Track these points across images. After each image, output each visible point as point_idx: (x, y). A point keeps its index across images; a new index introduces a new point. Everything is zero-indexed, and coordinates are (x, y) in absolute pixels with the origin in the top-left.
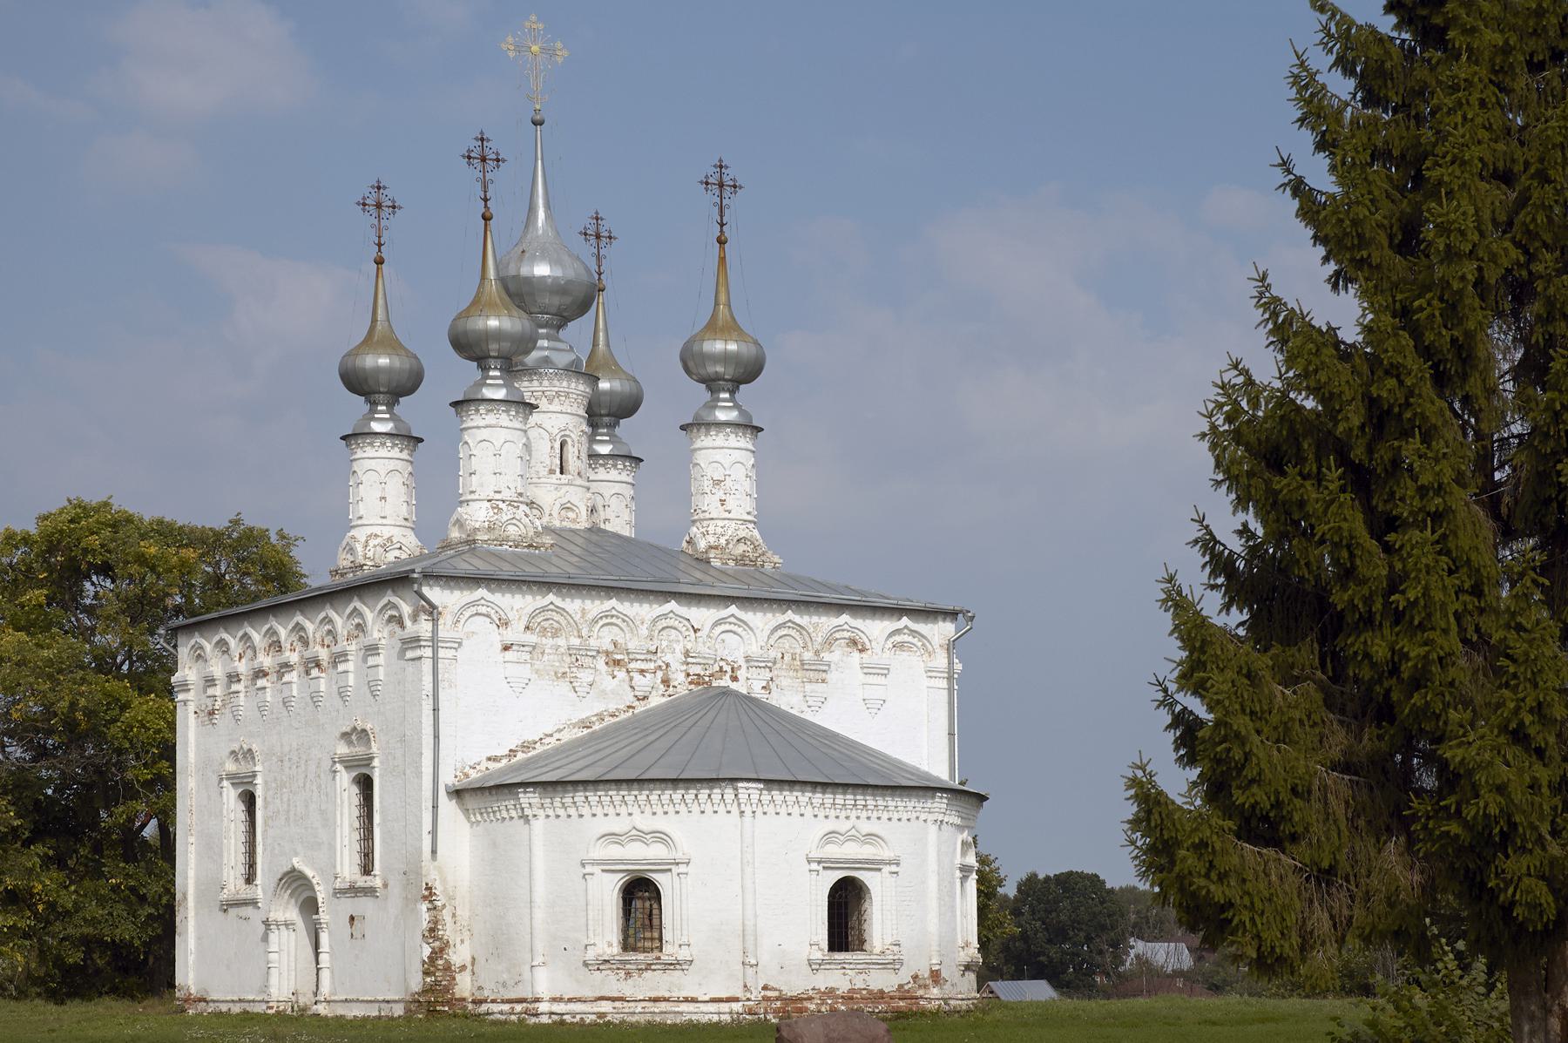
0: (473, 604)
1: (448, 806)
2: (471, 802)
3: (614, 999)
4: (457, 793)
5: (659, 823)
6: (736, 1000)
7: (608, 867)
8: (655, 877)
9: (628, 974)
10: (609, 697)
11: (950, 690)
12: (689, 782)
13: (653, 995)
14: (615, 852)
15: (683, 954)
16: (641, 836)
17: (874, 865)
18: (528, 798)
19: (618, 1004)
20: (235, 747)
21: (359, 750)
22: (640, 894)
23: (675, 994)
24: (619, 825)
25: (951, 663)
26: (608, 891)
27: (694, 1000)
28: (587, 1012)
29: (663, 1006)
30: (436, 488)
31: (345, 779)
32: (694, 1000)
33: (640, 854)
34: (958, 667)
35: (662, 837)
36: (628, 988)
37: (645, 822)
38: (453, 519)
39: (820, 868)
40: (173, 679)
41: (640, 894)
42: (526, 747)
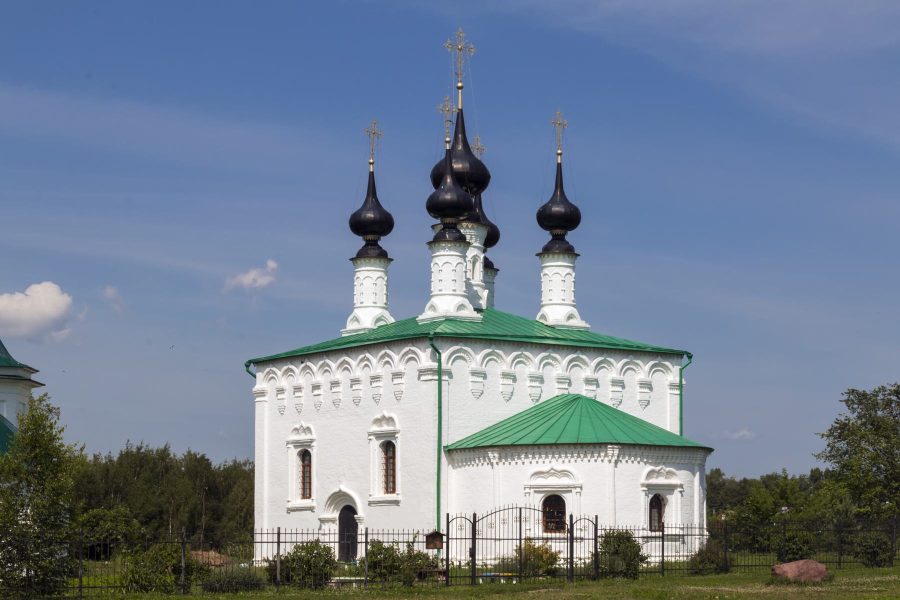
2: (457, 456)
5: (566, 467)
7: (537, 489)
10: (523, 400)
11: (681, 395)
14: (540, 481)
17: (671, 488)
18: (493, 455)
20: (298, 426)
21: (386, 428)
25: (681, 381)
26: (537, 501)
30: (411, 288)
31: (376, 444)
33: (554, 482)
34: (684, 382)
35: (565, 473)
38: (428, 305)
40: (254, 390)
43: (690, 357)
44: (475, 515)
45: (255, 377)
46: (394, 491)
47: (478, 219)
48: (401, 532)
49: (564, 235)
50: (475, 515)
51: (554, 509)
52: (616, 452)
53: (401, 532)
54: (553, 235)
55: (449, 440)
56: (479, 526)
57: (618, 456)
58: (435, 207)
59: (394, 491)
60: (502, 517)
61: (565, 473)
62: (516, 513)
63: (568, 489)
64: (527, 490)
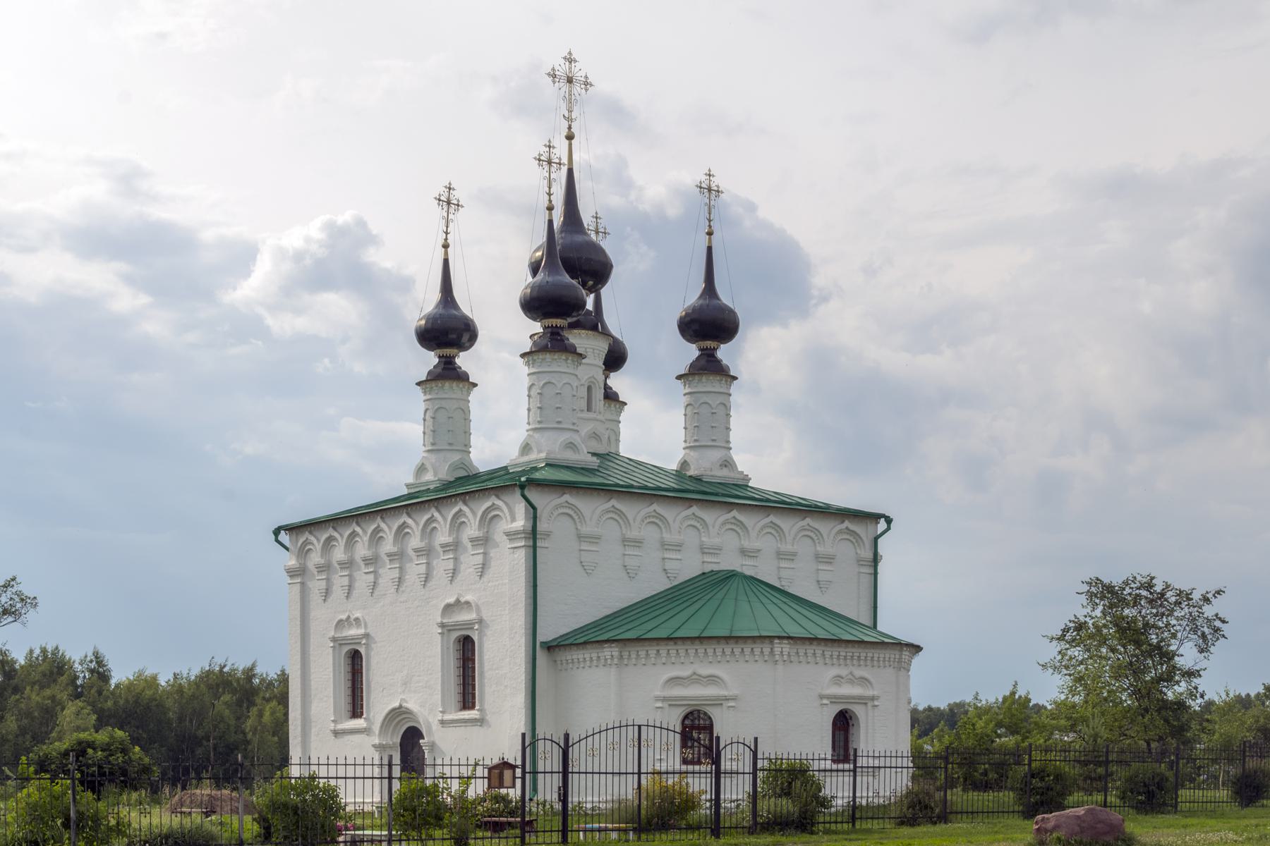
0: (561, 506)
1: (541, 656)
4: (550, 647)
7: (672, 702)
12: (737, 639)
16: (695, 679)
17: (863, 701)
22: (843, 723)
24: (685, 672)
26: (674, 719)
35: (713, 680)
37: (705, 670)
39: (666, 705)
41: (843, 723)
43: (889, 521)
44: (567, 736)
46: (473, 707)
47: (595, 323)
48: (360, 761)
49: (715, 349)
50: (567, 736)
51: (697, 733)
53: (360, 761)
54: (700, 350)
55: (546, 634)
56: (574, 753)
58: (535, 305)
59: (473, 707)
60: (610, 740)
61: (713, 680)
62: (632, 733)
63: (719, 702)
64: (659, 704)
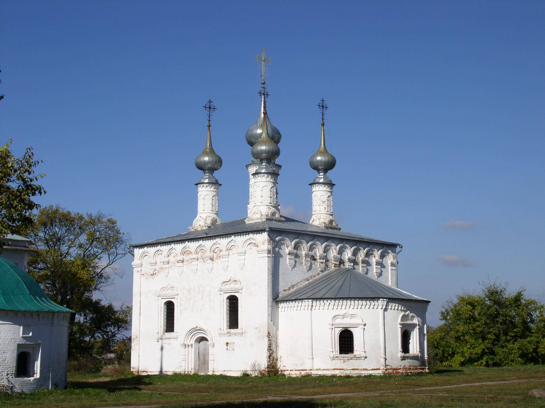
3: (340, 369)
6: (379, 369)
8: (352, 330)
9: (344, 361)
13: (353, 368)
14: (339, 321)
15: (363, 354)
18: (307, 303)
19: (341, 371)
23: (360, 368)
24: (343, 312)
27: (366, 370)
28: (329, 373)
29: (356, 372)
32: (366, 370)
33: (346, 322)
35: (352, 316)
36: (344, 366)
37: (351, 311)
40: (133, 263)
42: (293, 287)
45: (133, 255)
52: (385, 303)
57: (386, 306)
61: (352, 316)
